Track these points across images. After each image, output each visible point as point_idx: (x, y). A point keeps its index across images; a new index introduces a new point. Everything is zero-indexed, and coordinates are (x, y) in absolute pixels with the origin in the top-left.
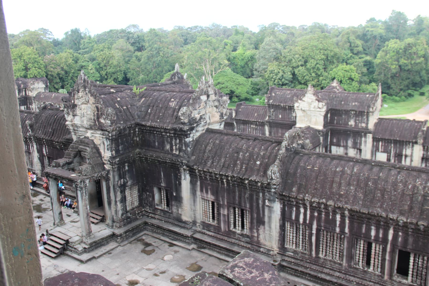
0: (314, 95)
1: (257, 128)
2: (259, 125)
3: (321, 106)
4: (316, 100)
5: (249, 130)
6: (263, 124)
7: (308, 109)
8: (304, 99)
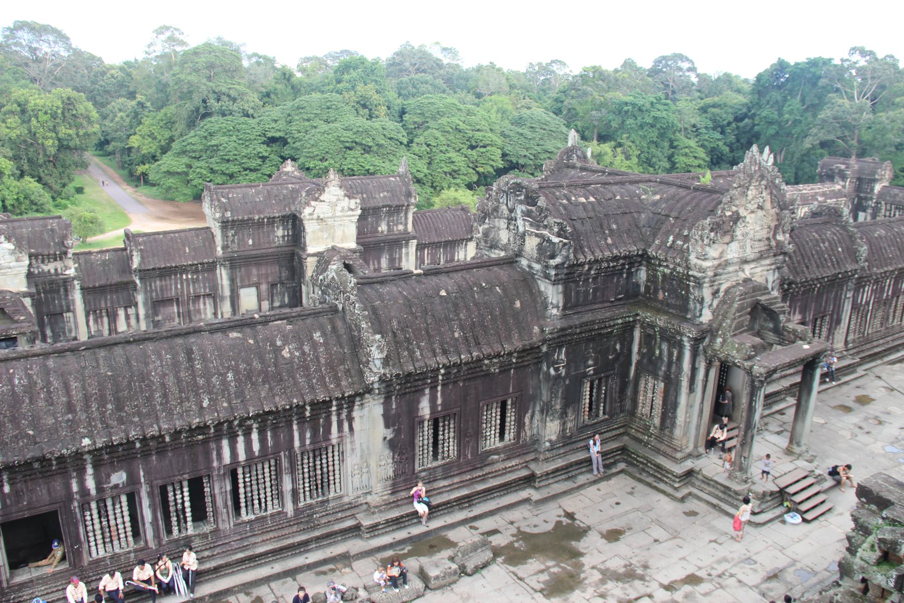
0: (341, 187)
1: (197, 278)
2: (203, 271)
3: (353, 207)
4: (346, 195)
5: (176, 288)
6: (211, 267)
7: (330, 215)
8: (322, 198)
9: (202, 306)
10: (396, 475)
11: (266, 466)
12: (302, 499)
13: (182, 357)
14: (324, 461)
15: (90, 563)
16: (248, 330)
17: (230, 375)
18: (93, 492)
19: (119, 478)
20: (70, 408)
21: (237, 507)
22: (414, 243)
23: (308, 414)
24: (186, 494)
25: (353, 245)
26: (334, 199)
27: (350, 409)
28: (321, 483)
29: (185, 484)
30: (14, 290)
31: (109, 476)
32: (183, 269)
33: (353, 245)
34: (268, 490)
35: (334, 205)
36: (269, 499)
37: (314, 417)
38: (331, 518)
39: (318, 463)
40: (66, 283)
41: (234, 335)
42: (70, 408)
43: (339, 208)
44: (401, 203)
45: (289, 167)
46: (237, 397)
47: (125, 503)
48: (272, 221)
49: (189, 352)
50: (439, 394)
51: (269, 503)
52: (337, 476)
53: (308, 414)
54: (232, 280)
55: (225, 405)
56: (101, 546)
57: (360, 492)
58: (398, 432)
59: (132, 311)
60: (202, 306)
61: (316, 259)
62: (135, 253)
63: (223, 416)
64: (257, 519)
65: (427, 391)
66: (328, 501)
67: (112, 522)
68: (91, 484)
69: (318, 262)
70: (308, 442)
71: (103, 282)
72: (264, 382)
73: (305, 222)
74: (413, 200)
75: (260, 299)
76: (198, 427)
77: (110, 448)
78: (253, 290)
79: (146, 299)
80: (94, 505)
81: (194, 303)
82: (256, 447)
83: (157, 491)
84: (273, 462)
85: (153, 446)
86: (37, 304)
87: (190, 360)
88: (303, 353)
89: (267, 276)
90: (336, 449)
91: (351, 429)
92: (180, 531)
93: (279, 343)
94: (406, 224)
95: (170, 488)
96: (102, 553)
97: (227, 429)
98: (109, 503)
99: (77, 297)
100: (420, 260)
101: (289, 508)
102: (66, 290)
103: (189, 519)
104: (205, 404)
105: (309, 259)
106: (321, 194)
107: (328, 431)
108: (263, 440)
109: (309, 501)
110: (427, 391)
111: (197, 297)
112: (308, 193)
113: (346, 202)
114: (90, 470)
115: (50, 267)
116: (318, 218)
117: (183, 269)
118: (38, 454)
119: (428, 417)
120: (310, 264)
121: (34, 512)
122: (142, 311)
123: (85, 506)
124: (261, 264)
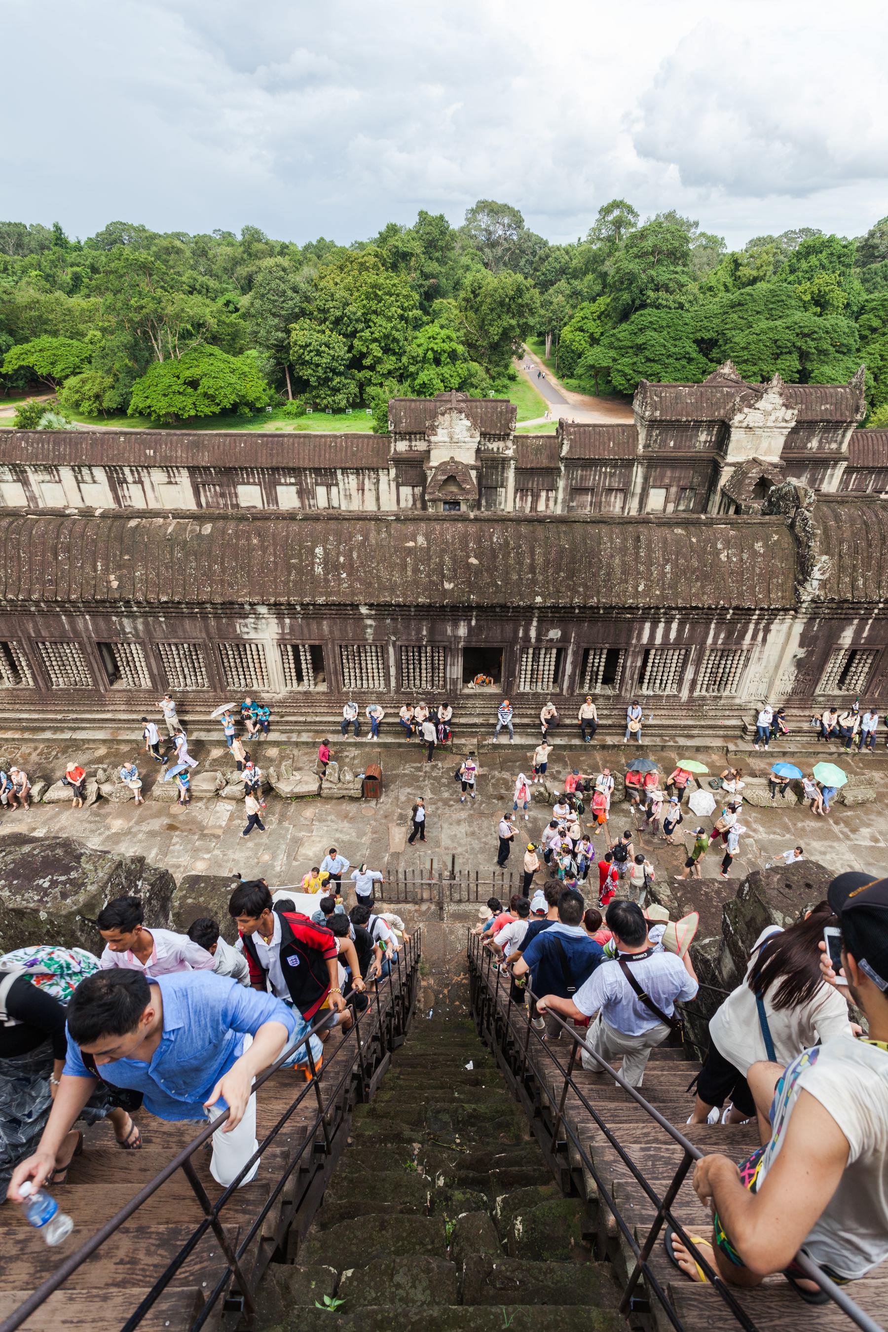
0: (781, 395)
1: (615, 473)
2: (622, 466)
3: (788, 418)
4: (784, 405)
6: (628, 464)
7: (761, 424)
8: (757, 406)
9: (613, 499)
10: (794, 692)
11: (677, 653)
12: (698, 689)
13: (630, 543)
14: (729, 662)
15: (518, 694)
16: (692, 529)
17: (668, 568)
18: (533, 640)
19: (555, 634)
20: (532, 569)
21: (641, 681)
22: (845, 464)
23: (728, 617)
24: (603, 660)
25: (775, 459)
26: (769, 407)
27: (770, 622)
28: (720, 680)
29: (605, 651)
30: (465, 462)
31: (548, 631)
32: (604, 462)
33: (775, 459)
34: (672, 674)
35: (767, 414)
36: (670, 682)
37: (733, 622)
38: (719, 713)
39: (723, 662)
40: (504, 462)
41: (679, 531)
42: (532, 569)
43: (773, 418)
44: (844, 419)
45: (727, 369)
46: (670, 587)
47: (554, 656)
48: (698, 424)
49: (638, 539)
50: (868, 627)
51: (669, 685)
52: (737, 679)
53: (728, 617)
54: (646, 479)
55: (658, 592)
56: (528, 684)
57: (753, 698)
58: (810, 654)
59: (552, 494)
60: (613, 499)
61: (733, 469)
62: (565, 442)
63: (653, 602)
64: (655, 696)
65: (856, 622)
66: (720, 697)
67: (541, 668)
68: (533, 633)
69: (735, 472)
70: (720, 642)
71: (534, 465)
72: (697, 580)
73: (732, 430)
74: (858, 417)
75: (667, 501)
76: (630, 608)
77: (555, 608)
78: (663, 492)
79: (567, 486)
80: (531, 651)
81: (606, 495)
82: (673, 635)
83: (581, 652)
84: (683, 652)
85: (589, 614)
86: (480, 477)
87: (637, 547)
88: (742, 560)
89: (680, 479)
90: (745, 653)
91: (764, 640)
92: (590, 688)
93: (720, 546)
94: (841, 443)
95: (592, 652)
96: (527, 689)
97: (652, 614)
98: (543, 652)
99: (511, 474)
100: (844, 483)
101: (685, 694)
102: (503, 468)
103: (600, 681)
104: (640, 589)
105: (726, 469)
106: (757, 401)
107: (742, 636)
108: (680, 631)
109: (704, 693)
110: (856, 622)
111: (610, 490)
112: (743, 399)
113: (782, 413)
114: (535, 623)
115: (494, 446)
116: (748, 427)
117: (604, 462)
118: (502, 601)
119: (846, 647)
120: (726, 474)
121: (489, 645)
122: (561, 496)
123: (524, 650)
124: (676, 467)
